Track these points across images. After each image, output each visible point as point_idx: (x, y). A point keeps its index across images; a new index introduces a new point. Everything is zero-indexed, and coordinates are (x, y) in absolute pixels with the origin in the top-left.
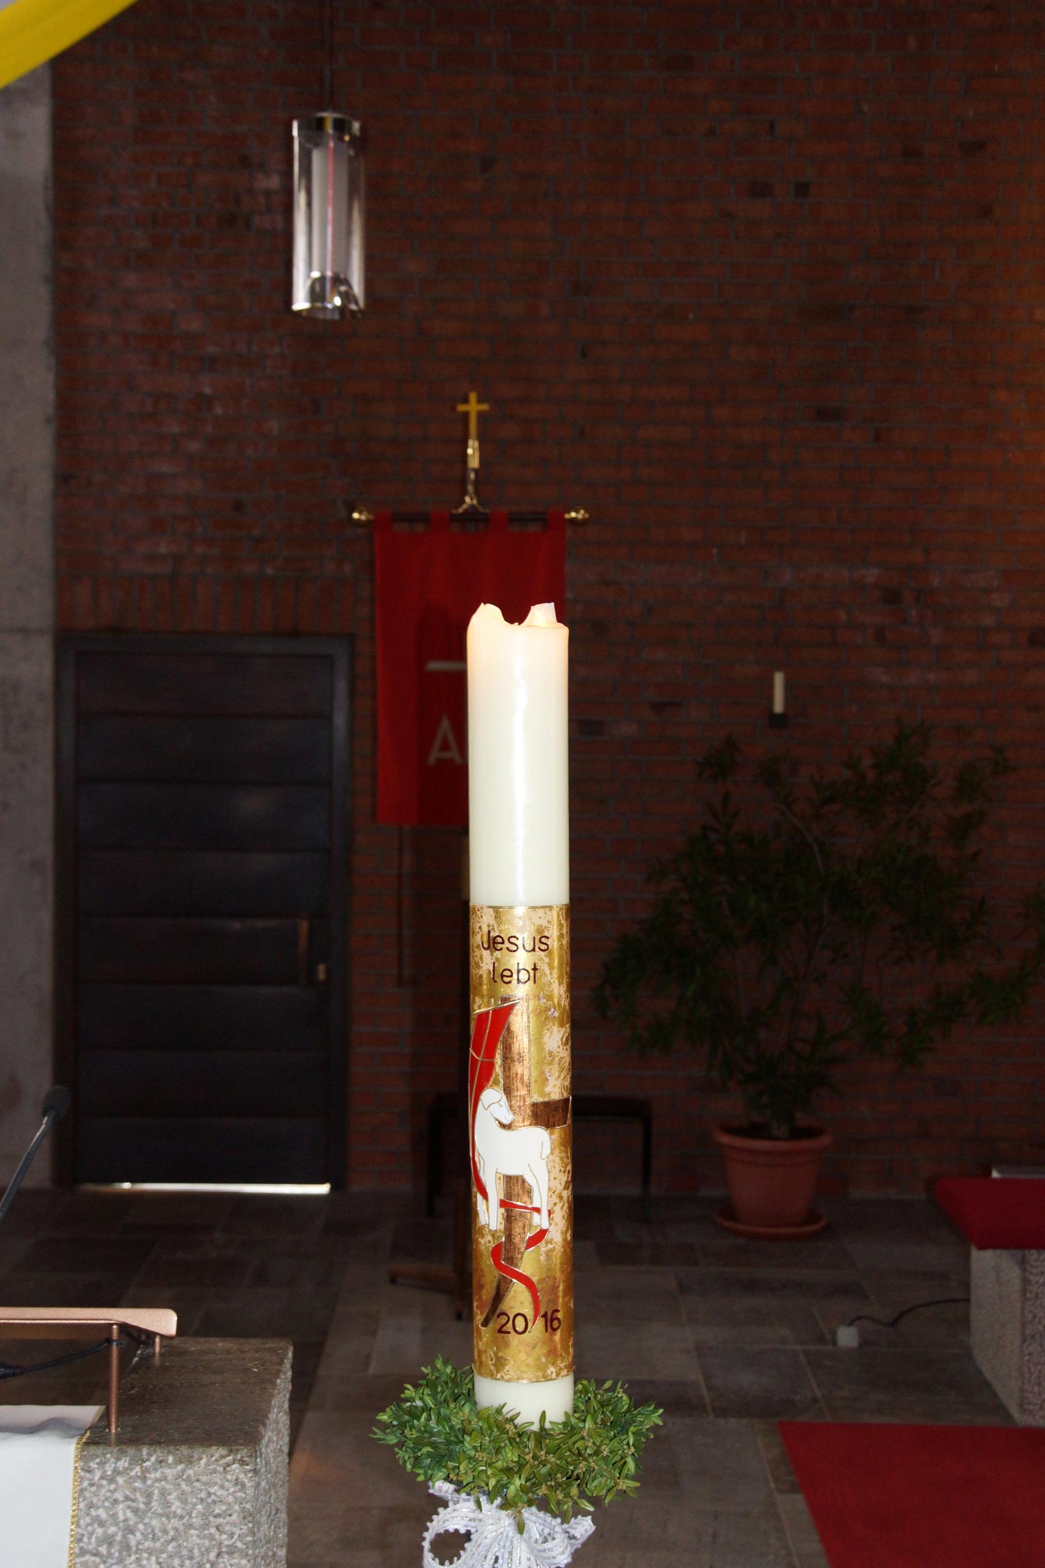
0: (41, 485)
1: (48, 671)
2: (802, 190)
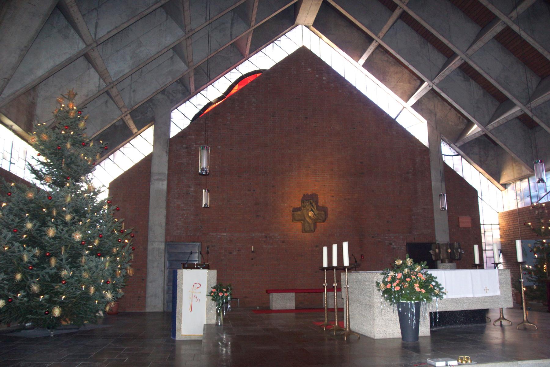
0: (164, 224)
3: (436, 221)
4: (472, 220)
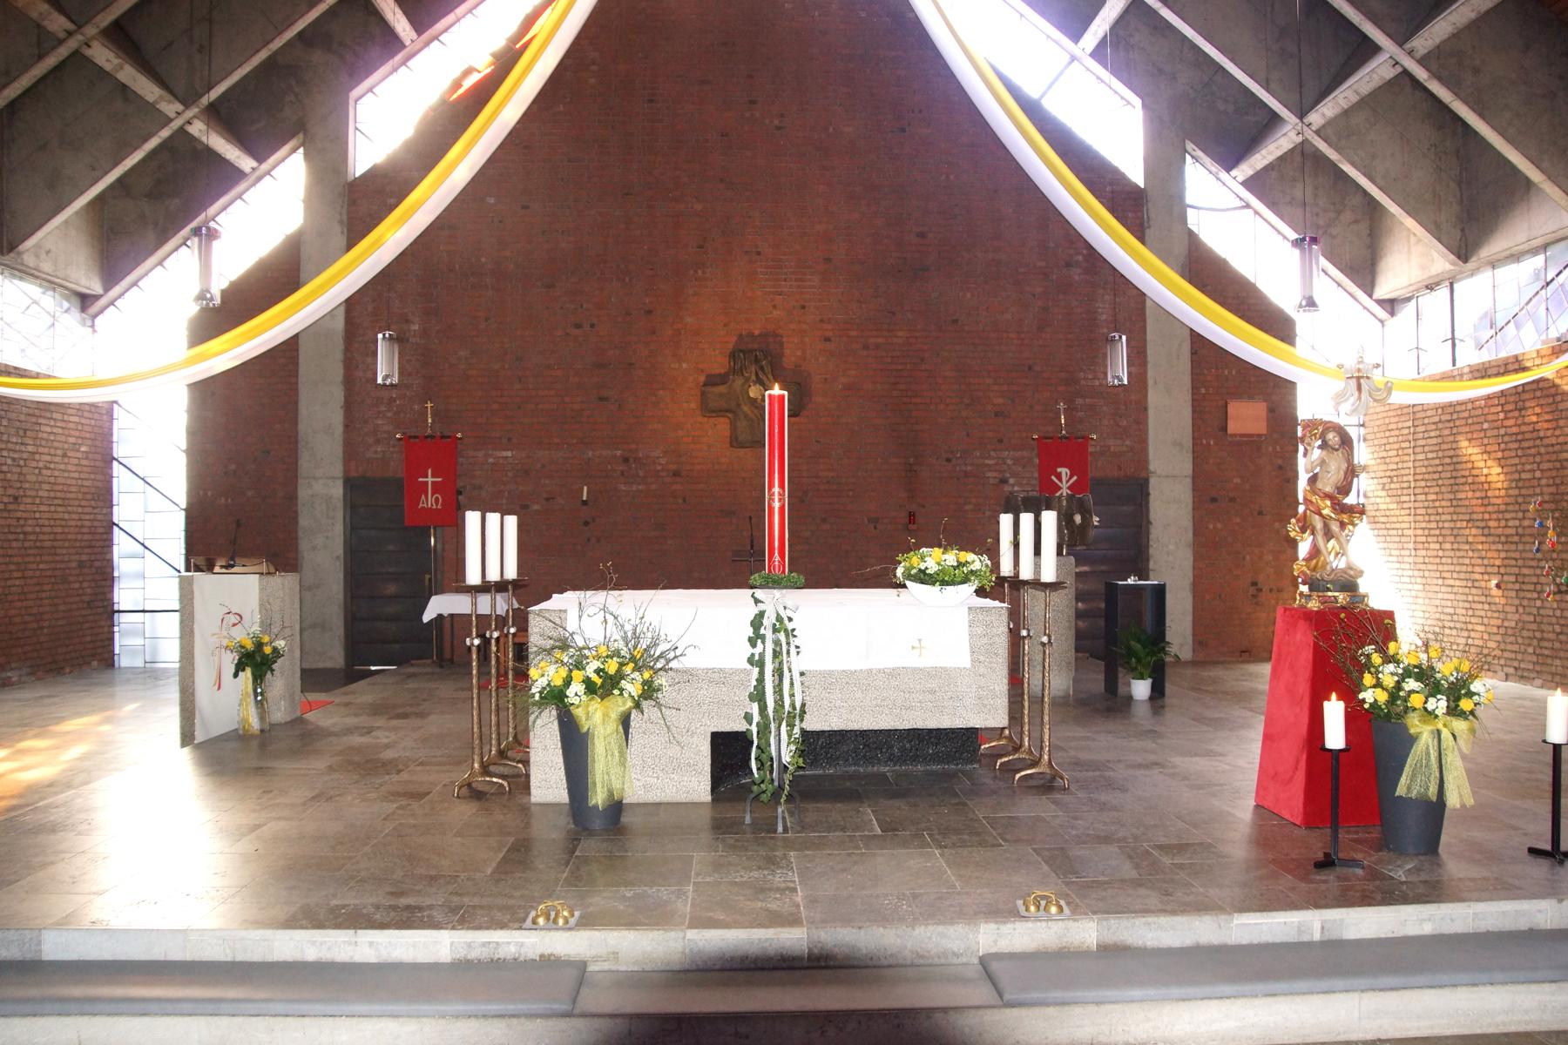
0: (339, 429)
1: (341, 491)
2: (592, 326)
3: (1151, 412)
4: (1271, 410)
